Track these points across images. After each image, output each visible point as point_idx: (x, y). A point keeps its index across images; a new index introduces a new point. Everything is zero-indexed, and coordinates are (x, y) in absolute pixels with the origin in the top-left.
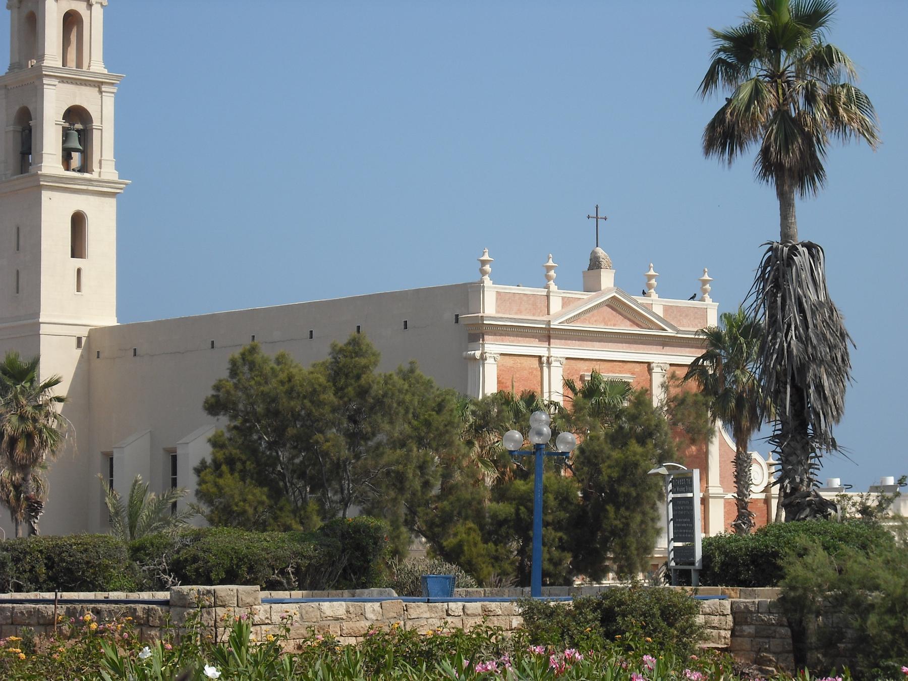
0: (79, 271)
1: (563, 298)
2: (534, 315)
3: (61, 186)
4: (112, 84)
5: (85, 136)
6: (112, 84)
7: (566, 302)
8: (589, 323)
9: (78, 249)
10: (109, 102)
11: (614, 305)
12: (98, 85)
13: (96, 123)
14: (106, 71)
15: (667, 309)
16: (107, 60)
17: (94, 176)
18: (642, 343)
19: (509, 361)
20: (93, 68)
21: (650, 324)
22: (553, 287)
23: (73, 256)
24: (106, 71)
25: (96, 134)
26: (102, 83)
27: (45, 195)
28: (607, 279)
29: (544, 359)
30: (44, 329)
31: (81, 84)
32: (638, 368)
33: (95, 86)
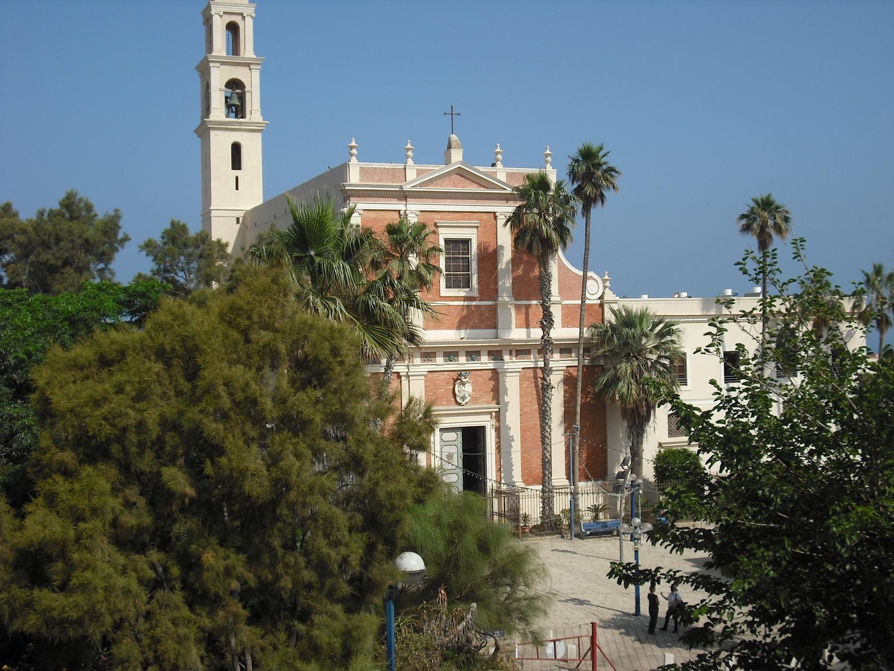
0: (237, 178)
1: (417, 170)
2: (393, 182)
3: (222, 127)
4: (259, 64)
5: (242, 98)
6: (259, 64)
7: (420, 173)
8: (441, 186)
9: (236, 163)
10: (256, 75)
11: (461, 173)
12: (248, 65)
13: (247, 88)
14: (255, 57)
15: (509, 175)
16: (256, 51)
17: (247, 120)
18: (487, 199)
19: (373, 215)
20: (247, 55)
21: (495, 187)
22: (410, 162)
23: (233, 169)
24: (255, 57)
25: (248, 95)
26: (251, 64)
27: (213, 134)
28: (457, 156)
29: (402, 212)
30: (213, 213)
31: (237, 65)
32: (485, 216)
33: (246, 66)
